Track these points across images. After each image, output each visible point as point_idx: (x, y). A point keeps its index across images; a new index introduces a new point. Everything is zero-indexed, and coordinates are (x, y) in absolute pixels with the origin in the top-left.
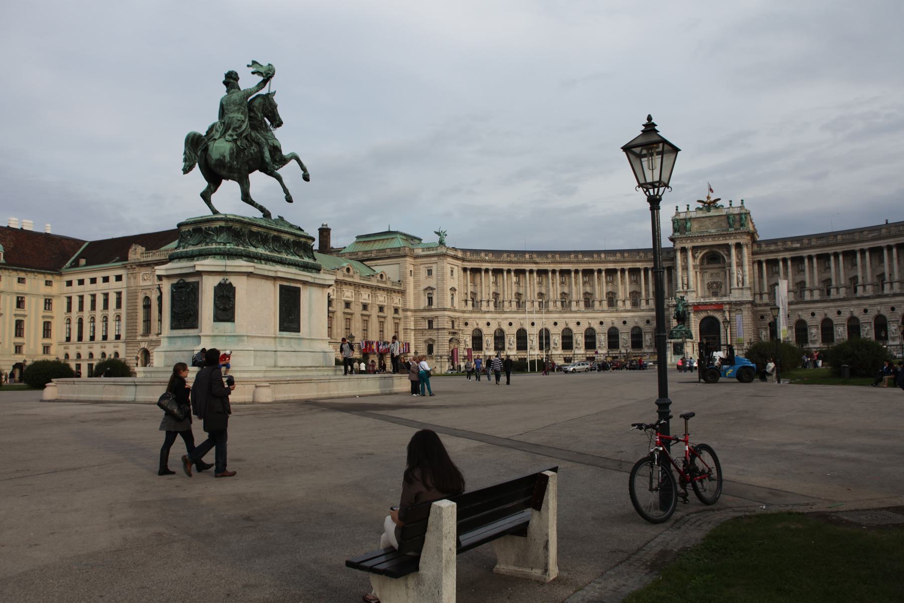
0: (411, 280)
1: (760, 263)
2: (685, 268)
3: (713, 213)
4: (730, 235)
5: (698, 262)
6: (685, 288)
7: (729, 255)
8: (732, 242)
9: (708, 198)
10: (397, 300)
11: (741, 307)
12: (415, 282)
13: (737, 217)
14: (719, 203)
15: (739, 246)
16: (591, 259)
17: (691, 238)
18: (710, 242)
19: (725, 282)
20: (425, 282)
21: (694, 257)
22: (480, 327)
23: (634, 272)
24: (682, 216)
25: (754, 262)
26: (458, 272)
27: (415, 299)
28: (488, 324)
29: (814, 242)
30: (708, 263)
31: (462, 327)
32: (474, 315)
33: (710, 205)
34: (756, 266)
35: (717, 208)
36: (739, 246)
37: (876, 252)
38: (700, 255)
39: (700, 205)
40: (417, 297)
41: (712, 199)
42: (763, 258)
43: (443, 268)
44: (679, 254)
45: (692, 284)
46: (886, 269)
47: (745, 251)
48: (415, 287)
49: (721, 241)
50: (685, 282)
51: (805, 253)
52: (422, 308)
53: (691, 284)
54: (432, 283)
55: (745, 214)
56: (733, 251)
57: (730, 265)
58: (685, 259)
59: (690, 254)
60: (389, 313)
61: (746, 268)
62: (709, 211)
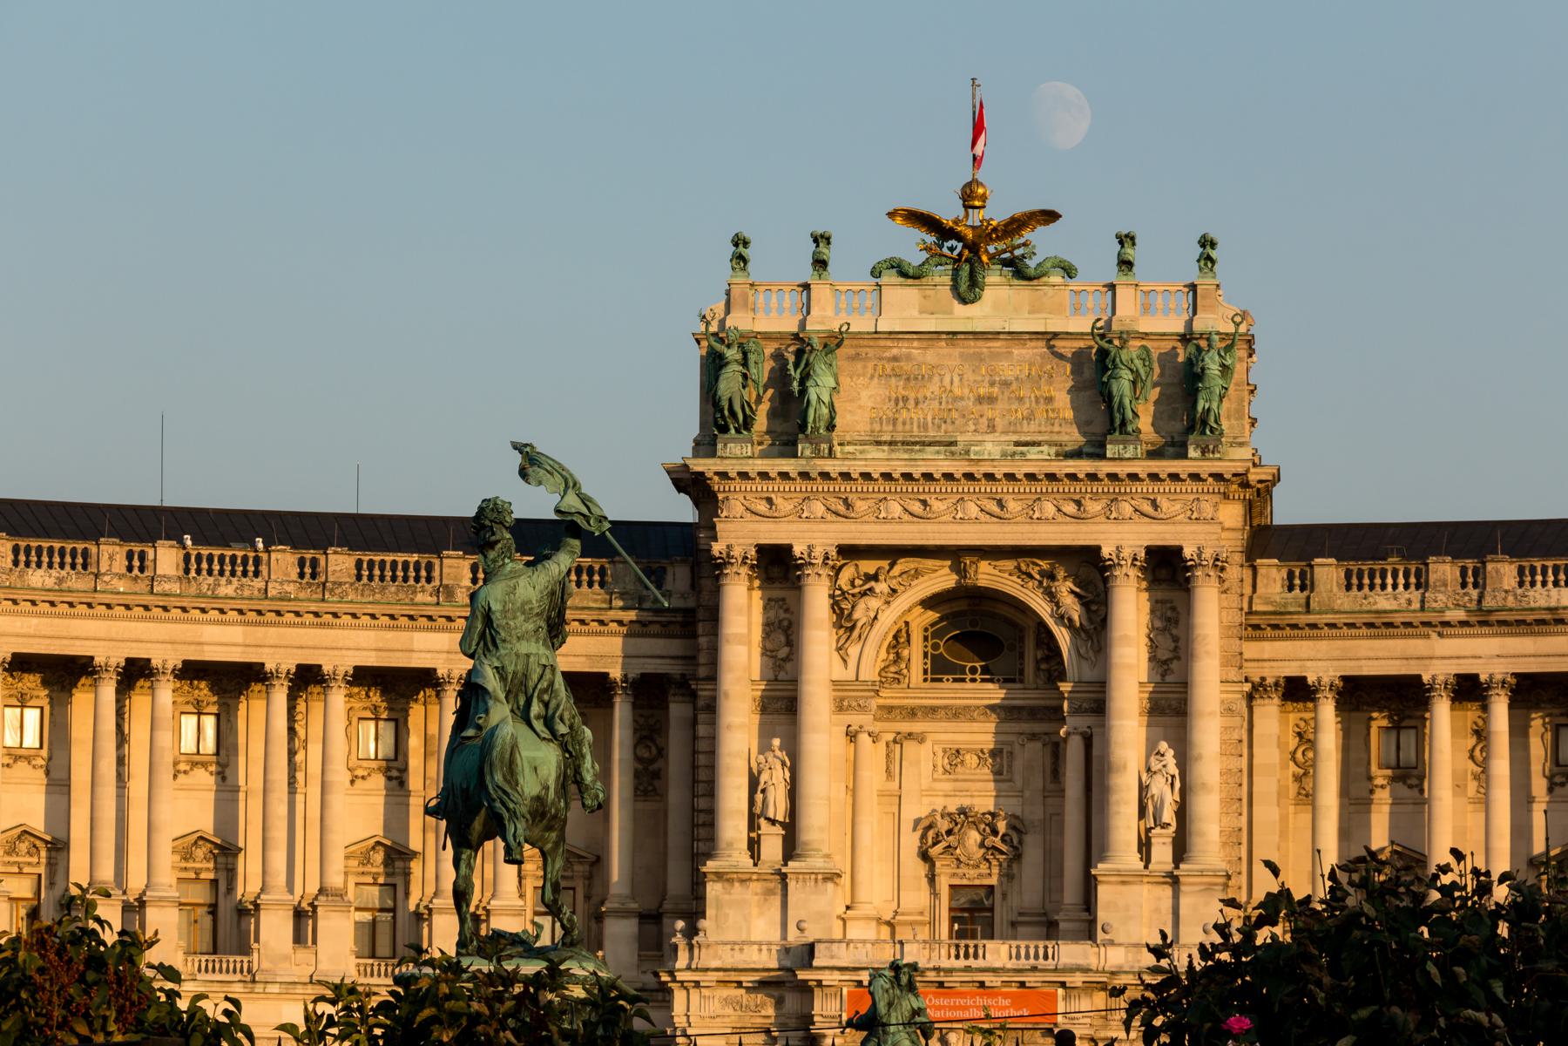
3: (999, 306)
5: (870, 656)
6: (772, 846)
7: (1096, 628)
8: (1123, 537)
9: (969, 196)
14: (1042, 243)
15: (1168, 570)
19: (1054, 821)
21: (844, 621)
24: (769, 317)
25: (1256, 691)
30: (939, 669)
33: (968, 249)
35: (1018, 269)
36: (1168, 570)
39: (911, 244)
41: (997, 212)
45: (818, 823)
47: (1212, 611)
50: (777, 805)
55: (1230, 342)
56: (1131, 609)
57: (1097, 704)
58: (784, 636)
61: (1210, 731)
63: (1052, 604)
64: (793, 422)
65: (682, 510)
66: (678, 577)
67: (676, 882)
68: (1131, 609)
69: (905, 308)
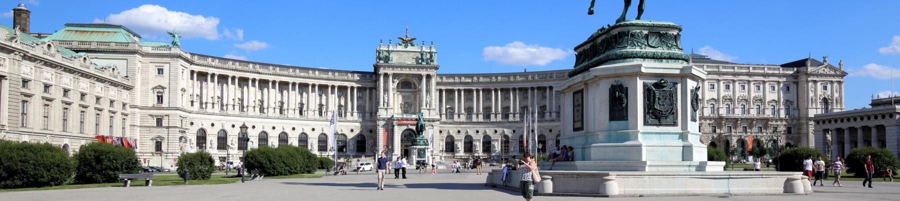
0: (139, 76)
1: (441, 91)
2: (386, 90)
3: (410, 48)
4: (423, 68)
8: (424, 73)
10: (125, 95)
12: (142, 79)
13: (428, 56)
16: (306, 75)
17: (393, 67)
18: (406, 71)
19: (415, 104)
20: (155, 80)
22: (204, 127)
23: (343, 89)
26: (187, 74)
29: (481, 79)
31: (189, 126)
34: (438, 93)
35: (412, 45)
37: (524, 90)
38: (397, 81)
39: (400, 41)
42: (443, 88)
43: (177, 69)
44: (382, 78)
47: (433, 81)
48: (143, 84)
49: (415, 72)
51: (456, 88)
52: (150, 105)
53: (392, 104)
54: (163, 81)
56: (424, 80)
57: (420, 91)
58: (386, 82)
59: (391, 78)
60: (118, 107)
62: (406, 47)
63: (415, 81)
64: (387, 59)
65: (373, 71)
67: (374, 109)
68: (424, 80)
69: (400, 48)
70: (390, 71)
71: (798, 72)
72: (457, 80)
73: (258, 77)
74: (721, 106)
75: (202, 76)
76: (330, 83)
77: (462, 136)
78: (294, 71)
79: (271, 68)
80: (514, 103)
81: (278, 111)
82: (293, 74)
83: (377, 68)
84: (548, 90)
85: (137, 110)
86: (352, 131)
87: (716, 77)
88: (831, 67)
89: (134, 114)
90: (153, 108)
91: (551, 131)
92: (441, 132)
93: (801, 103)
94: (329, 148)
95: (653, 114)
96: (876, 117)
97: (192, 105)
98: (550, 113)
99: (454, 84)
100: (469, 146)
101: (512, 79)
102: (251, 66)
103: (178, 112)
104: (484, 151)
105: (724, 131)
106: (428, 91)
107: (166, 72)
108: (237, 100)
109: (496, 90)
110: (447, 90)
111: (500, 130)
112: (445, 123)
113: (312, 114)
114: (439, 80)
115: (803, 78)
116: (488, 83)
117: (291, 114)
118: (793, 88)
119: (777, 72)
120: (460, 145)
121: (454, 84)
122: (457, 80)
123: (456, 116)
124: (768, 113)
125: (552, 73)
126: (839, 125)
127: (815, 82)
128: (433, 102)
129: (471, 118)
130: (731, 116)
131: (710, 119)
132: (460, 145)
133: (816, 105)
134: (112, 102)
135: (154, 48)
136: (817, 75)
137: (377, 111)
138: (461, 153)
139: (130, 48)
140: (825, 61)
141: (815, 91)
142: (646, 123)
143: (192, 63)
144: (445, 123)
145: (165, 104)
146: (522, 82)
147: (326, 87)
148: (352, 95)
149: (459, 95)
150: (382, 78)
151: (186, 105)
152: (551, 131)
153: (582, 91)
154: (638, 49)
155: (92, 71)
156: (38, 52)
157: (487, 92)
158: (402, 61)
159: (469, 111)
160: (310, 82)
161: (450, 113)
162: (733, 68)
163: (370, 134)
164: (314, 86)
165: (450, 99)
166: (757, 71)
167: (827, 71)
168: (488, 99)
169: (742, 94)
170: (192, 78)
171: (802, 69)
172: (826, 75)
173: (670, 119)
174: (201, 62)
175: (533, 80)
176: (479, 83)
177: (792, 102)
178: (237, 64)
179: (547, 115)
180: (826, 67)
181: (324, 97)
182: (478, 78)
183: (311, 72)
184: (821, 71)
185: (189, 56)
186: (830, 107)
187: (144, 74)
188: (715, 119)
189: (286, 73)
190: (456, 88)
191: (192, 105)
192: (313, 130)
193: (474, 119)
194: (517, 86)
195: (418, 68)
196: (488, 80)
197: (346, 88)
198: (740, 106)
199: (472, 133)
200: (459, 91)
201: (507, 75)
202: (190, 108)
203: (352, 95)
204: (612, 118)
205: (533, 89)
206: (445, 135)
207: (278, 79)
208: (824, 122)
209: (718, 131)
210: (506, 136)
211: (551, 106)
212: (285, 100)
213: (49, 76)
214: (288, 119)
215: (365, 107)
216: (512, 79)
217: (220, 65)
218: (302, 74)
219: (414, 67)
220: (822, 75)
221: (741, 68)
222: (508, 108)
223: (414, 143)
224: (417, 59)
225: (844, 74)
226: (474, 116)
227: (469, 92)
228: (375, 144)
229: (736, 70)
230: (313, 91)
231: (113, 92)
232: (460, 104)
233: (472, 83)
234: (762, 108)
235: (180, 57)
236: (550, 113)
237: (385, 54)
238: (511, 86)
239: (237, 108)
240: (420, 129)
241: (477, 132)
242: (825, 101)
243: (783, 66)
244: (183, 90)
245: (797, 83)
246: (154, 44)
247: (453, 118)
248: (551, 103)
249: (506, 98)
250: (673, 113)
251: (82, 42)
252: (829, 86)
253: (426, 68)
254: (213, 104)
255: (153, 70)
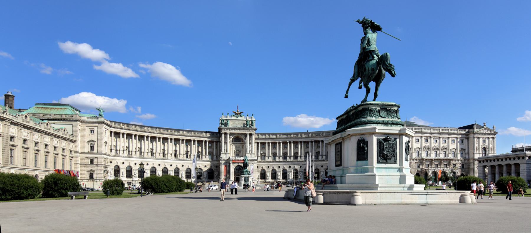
0: (79, 135)
1: (258, 143)
2: (226, 143)
3: (239, 118)
4: (247, 129)
8: (248, 132)
10: (71, 146)
11: (253, 162)
13: (250, 123)
16: (179, 134)
17: (230, 129)
19: (243, 151)
20: (89, 137)
22: (119, 164)
23: (200, 142)
26: (108, 133)
27: (81, 146)
28: (123, 163)
29: (282, 136)
32: (115, 158)
34: (256, 144)
35: (241, 116)
37: (306, 143)
38: (232, 137)
39: (234, 114)
40: (83, 145)
42: (259, 141)
44: (223, 136)
46: (310, 150)
47: (253, 137)
48: (82, 139)
49: (243, 132)
53: (229, 151)
54: (94, 137)
56: (248, 137)
57: (246, 143)
58: (225, 138)
59: (228, 136)
61: (253, 145)
63: (242, 137)
64: (226, 124)
65: (217, 131)
66: (218, 135)
67: (218, 154)
68: (248, 137)
69: (234, 118)
70: (228, 132)
71: (468, 132)
72: (267, 136)
73: (149, 135)
74: (423, 152)
75: (117, 134)
76: (192, 138)
77: (270, 170)
78: (171, 131)
79: (158, 129)
80: (301, 150)
81: (162, 155)
82: (171, 133)
83: (220, 129)
84: (321, 143)
85: (78, 154)
86: (206, 166)
87: (420, 135)
88: (488, 129)
89: (77, 156)
90: (88, 153)
91: (322, 166)
92: (258, 167)
93: (470, 150)
94: (192, 177)
95: (382, 156)
96: (514, 159)
97: (111, 151)
98: (322, 156)
99: (266, 139)
100: (274, 175)
101: (299, 136)
102: (146, 128)
103: (103, 155)
104: (283, 178)
105: (424, 167)
106: (250, 143)
107: (95, 132)
108: (137, 149)
109: (290, 143)
110: (261, 143)
111: (292, 166)
112: (260, 162)
113: (182, 156)
114: (257, 136)
115: (471, 136)
116: (285, 138)
117: (169, 157)
118: (465, 141)
119: (456, 132)
120: (269, 175)
121: (266, 139)
122: (267, 136)
123: (267, 158)
124: (451, 156)
125: (323, 132)
126: (493, 163)
127: (479, 138)
128: (253, 149)
129: (275, 159)
130: (429, 158)
131: (416, 160)
132: (269, 175)
133: (479, 151)
134: (63, 150)
135: (88, 118)
136: (480, 134)
137: (220, 155)
138: (270, 179)
139: (74, 117)
140: (485, 125)
141: (479, 143)
142: (378, 162)
143: (111, 127)
144: (260, 162)
145: (95, 151)
146: (306, 138)
147: (190, 140)
148: (206, 146)
149: (269, 146)
150: (223, 136)
151: (107, 151)
152: (322, 166)
153: (340, 143)
154: (374, 119)
155: (52, 131)
156: (19, 120)
157: (285, 143)
158: (235, 125)
159: (274, 155)
160: (181, 138)
161: (263, 156)
162: (430, 129)
163: (216, 168)
164: (183, 140)
165: (263, 148)
166: (444, 131)
167: (486, 131)
168: (285, 148)
169: (435, 145)
170: (111, 136)
171: (471, 130)
172: (485, 134)
173: (393, 160)
174: (116, 126)
175: (312, 137)
176: (280, 138)
177: (464, 150)
178: (138, 127)
179: (320, 157)
180: (485, 129)
181: (189, 146)
182: (280, 135)
183: (181, 132)
184: (482, 132)
185: (109, 123)
186: (487, 153)
187: (83, 134)
188: (419, 160)
189: (166, 132)
190: (267, 141)
191: (111, 151)
192: (183, 166)
193: (277, 159)
194: (302, 140)
195: (244, 129)
196: (285, 136)
197: (202, 141)
198: (434, 152)
199: (276, 167)
200: (269, 143)
201: (297, 134)
202: (110, 153)
203: (206, 146)
204: (358, 159)
205: (312, 142)
206: (260, 169)
207: (162, 136)
208: (483, 162)
209: (421, 167)
210: (296, 170)
211: (322, 152)
212: (166, 148)
213: (26, 134)
214: (168, 159)
215: (213, 153)
216: (299, 136)
217: (127, 128)
218: (176, 133)
219: (242, 129)
220: (483, 134)
221: (435, 130)
222: (297, 153)
223: (242, 173)
224: (244, 124)
225: (495, 133)
226: (277, 158)
227: (274, 144)
228: (219, 174)
229: (432, 131)
230: (183, 143)
231: (64, 144)
232: (269, 151)
233: (276, 138)
234: (447, 153)
235: (103, 123)
236: (322, 156)
237: (225, 121)
238: (299, 140)
239: (138, 153)
240: (246, 165)
241: (279, 167)
242: (485, 149)
243: (460, 128)
244: (106, 143)
245: (468, 139)
246: (88, 115)
247: (265, 159)
248: (322, 150)
249: (296, 147)
250: (395, 156)
251: (46, 114)
252: (487, 140)
253: (249, 130)
254: (124, 151)
255: (87, 131)
